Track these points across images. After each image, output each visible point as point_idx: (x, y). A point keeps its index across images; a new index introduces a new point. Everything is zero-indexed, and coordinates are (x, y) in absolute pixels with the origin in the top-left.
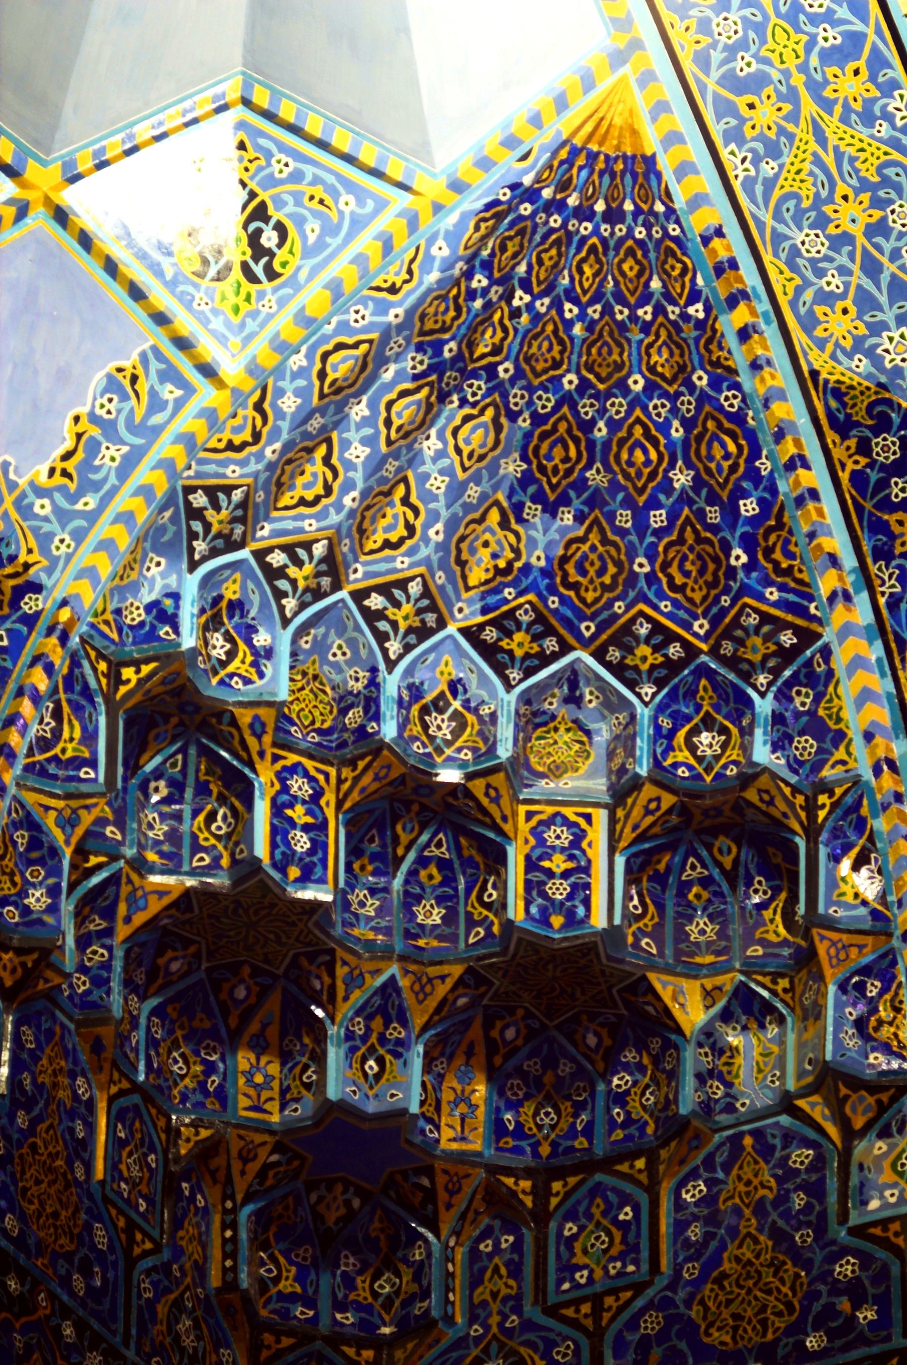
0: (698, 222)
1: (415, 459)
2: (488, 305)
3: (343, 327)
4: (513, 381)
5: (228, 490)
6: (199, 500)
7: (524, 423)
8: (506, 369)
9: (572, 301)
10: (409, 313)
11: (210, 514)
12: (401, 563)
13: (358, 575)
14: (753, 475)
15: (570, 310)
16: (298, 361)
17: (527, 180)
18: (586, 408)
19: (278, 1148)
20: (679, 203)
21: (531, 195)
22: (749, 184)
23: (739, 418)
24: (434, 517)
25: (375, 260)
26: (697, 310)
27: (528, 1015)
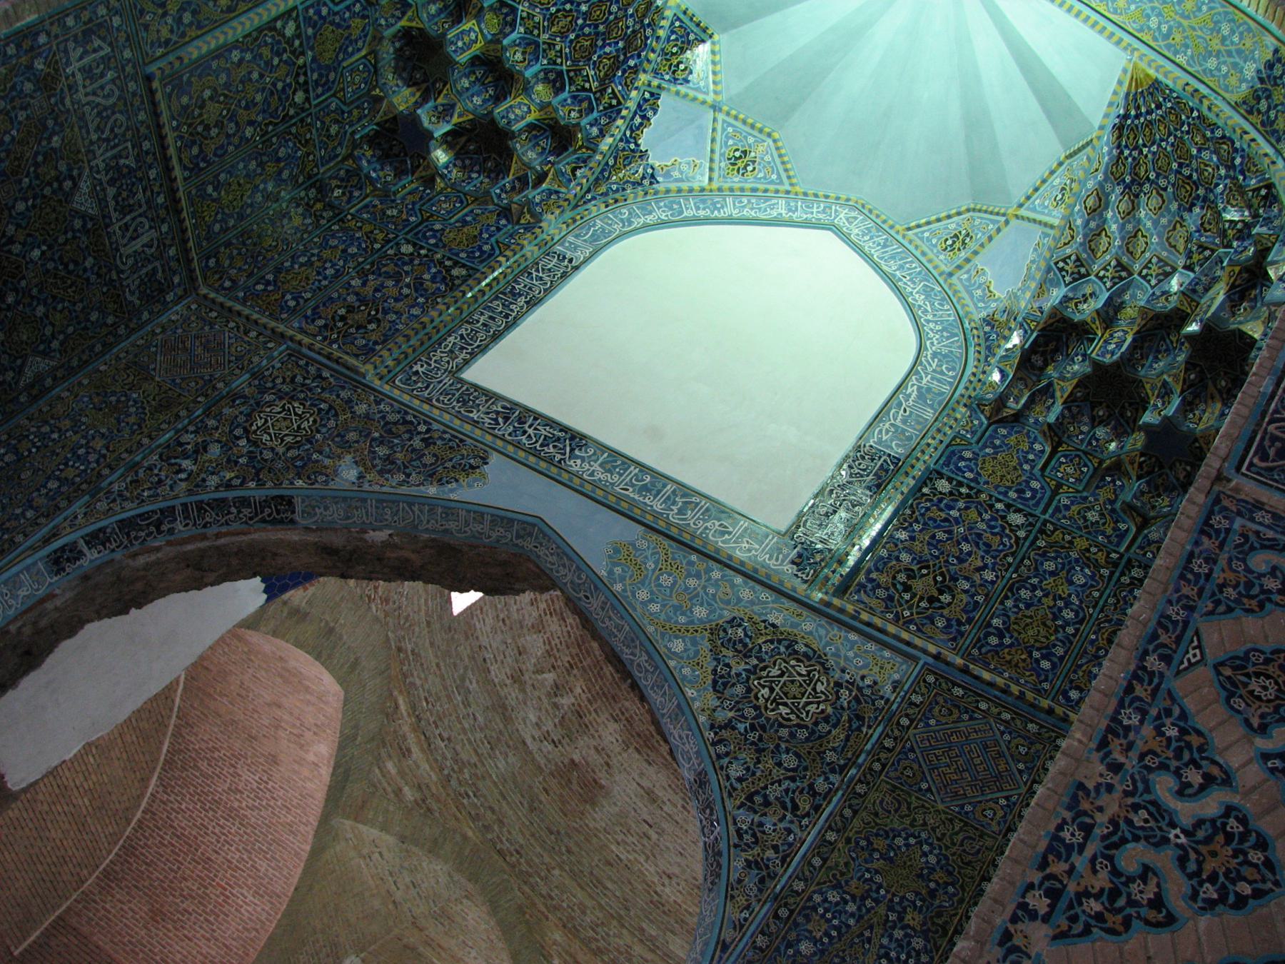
0: (1179, 88)
1: (1139, 221)
2: (1134, 159)
3: (1087, 190)
4: (1157, 177)
5: (1069, 257)
6: (1061, 264)
7: (1170, 189)
8: (1152, 176)
9: (1155, 140)
10: (1105, 173)
11: (1067, 268)
12: (1147, 255)
13: (1137, 267)
14: (1236, 150)
15: (1164, 144)
16: (1077, 208)
17: (1122, 112)
18: (1186, 172)
19: (1142, 455)
20: (1171, 86)
21: (1126, 116)
22: (1188, 64)
23: (1224, 137)
24: (1152, 235)
25: (1087, 165)
26: (1195, 114)
27: (1226, 373)
